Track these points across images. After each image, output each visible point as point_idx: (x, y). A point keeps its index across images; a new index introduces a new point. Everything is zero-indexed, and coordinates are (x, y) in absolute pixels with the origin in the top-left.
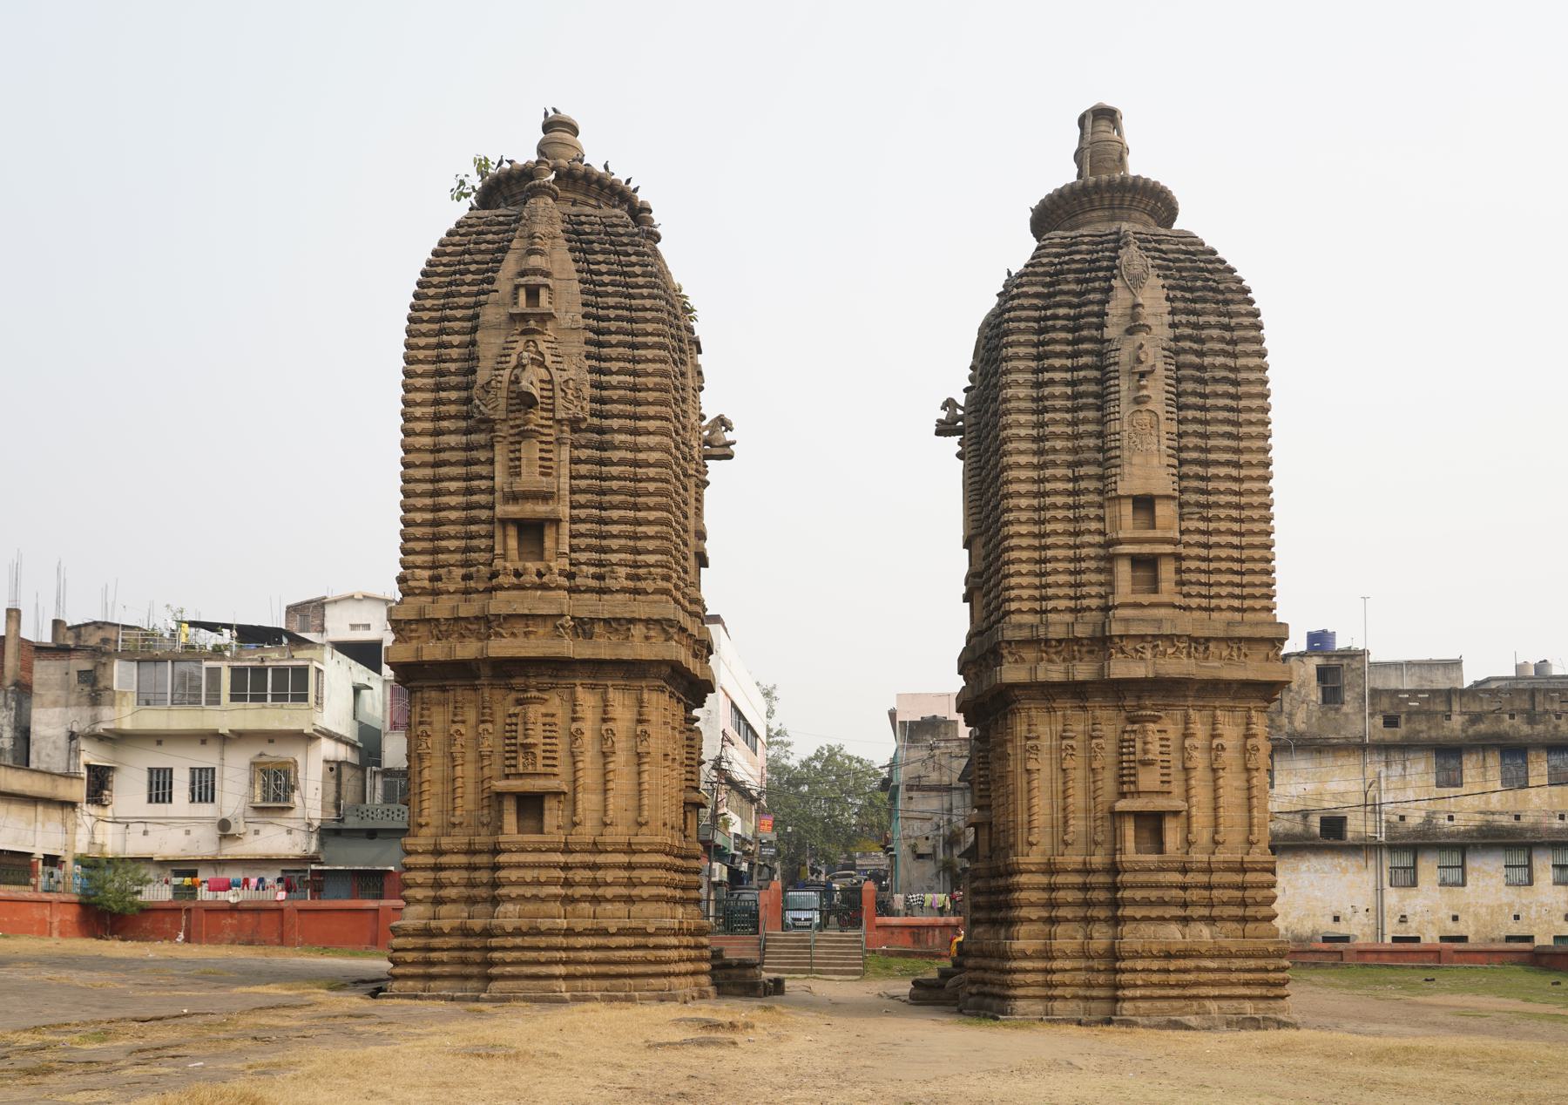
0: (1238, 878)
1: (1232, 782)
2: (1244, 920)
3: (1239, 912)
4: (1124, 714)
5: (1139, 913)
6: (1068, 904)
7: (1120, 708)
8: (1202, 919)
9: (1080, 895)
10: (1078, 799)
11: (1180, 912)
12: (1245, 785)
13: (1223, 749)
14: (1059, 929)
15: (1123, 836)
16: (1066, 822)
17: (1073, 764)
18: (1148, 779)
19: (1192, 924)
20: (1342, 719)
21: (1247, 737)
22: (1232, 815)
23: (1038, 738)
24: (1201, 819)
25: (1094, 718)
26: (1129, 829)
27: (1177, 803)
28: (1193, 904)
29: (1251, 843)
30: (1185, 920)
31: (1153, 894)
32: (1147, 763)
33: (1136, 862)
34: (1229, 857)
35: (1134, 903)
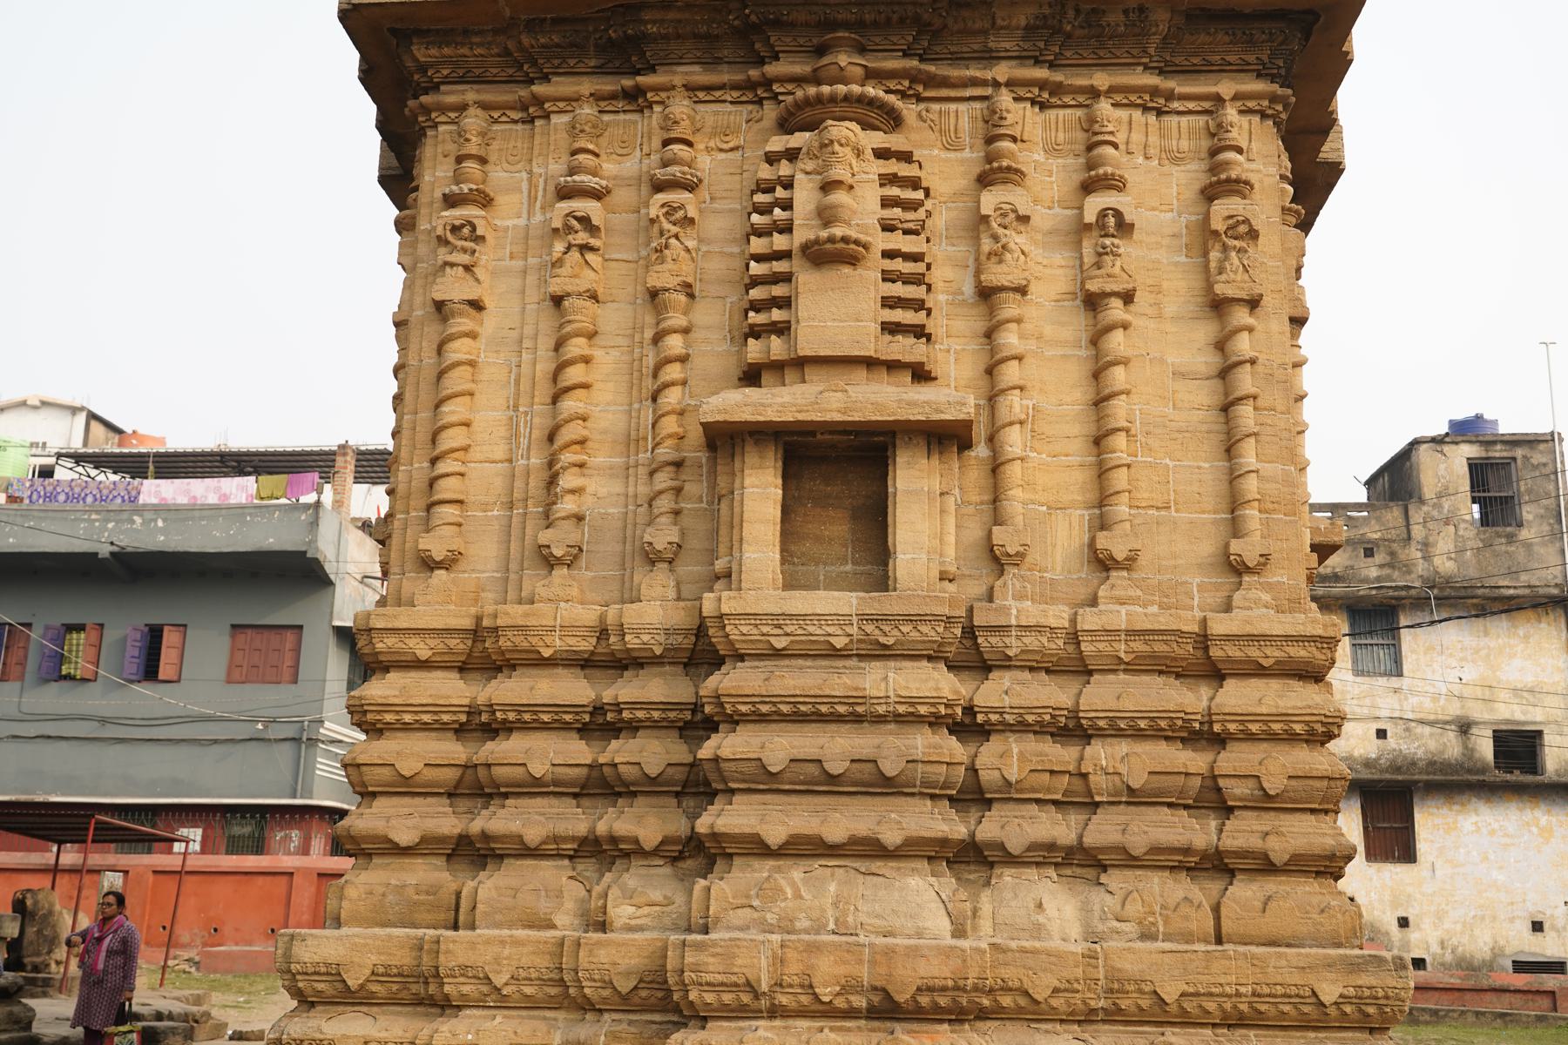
0: (1191, 699)
1: (1163, 349)
2: (1218, 865)
3: (1199, 832)
4: (770, 112)
5: (775, 820)
6: (533, 787)
7: (757, 91)
8: (1047, 856)
9: (578, 751)
10: (604, 403)
11: (949, 825)
13: (1125, 227)
14: (489, 886)
15: (736, 523)
16: (552, 481)
17: (587, 280)
18: (835, 312)
19: (1007, 877)
20: (1520, 554)
21: (1210, 194)
22: (1168, 469)
23: (485, 201)
25: (669, 122)
26: (761, 489)
27: (954, 396)
28: (1010, 794)
29: (1237, 569)
30: (972, 859)
31: (837, 747)
32: (830, 255)
33: (779, 620)
34: (1150, 616)
35: (764, 781)
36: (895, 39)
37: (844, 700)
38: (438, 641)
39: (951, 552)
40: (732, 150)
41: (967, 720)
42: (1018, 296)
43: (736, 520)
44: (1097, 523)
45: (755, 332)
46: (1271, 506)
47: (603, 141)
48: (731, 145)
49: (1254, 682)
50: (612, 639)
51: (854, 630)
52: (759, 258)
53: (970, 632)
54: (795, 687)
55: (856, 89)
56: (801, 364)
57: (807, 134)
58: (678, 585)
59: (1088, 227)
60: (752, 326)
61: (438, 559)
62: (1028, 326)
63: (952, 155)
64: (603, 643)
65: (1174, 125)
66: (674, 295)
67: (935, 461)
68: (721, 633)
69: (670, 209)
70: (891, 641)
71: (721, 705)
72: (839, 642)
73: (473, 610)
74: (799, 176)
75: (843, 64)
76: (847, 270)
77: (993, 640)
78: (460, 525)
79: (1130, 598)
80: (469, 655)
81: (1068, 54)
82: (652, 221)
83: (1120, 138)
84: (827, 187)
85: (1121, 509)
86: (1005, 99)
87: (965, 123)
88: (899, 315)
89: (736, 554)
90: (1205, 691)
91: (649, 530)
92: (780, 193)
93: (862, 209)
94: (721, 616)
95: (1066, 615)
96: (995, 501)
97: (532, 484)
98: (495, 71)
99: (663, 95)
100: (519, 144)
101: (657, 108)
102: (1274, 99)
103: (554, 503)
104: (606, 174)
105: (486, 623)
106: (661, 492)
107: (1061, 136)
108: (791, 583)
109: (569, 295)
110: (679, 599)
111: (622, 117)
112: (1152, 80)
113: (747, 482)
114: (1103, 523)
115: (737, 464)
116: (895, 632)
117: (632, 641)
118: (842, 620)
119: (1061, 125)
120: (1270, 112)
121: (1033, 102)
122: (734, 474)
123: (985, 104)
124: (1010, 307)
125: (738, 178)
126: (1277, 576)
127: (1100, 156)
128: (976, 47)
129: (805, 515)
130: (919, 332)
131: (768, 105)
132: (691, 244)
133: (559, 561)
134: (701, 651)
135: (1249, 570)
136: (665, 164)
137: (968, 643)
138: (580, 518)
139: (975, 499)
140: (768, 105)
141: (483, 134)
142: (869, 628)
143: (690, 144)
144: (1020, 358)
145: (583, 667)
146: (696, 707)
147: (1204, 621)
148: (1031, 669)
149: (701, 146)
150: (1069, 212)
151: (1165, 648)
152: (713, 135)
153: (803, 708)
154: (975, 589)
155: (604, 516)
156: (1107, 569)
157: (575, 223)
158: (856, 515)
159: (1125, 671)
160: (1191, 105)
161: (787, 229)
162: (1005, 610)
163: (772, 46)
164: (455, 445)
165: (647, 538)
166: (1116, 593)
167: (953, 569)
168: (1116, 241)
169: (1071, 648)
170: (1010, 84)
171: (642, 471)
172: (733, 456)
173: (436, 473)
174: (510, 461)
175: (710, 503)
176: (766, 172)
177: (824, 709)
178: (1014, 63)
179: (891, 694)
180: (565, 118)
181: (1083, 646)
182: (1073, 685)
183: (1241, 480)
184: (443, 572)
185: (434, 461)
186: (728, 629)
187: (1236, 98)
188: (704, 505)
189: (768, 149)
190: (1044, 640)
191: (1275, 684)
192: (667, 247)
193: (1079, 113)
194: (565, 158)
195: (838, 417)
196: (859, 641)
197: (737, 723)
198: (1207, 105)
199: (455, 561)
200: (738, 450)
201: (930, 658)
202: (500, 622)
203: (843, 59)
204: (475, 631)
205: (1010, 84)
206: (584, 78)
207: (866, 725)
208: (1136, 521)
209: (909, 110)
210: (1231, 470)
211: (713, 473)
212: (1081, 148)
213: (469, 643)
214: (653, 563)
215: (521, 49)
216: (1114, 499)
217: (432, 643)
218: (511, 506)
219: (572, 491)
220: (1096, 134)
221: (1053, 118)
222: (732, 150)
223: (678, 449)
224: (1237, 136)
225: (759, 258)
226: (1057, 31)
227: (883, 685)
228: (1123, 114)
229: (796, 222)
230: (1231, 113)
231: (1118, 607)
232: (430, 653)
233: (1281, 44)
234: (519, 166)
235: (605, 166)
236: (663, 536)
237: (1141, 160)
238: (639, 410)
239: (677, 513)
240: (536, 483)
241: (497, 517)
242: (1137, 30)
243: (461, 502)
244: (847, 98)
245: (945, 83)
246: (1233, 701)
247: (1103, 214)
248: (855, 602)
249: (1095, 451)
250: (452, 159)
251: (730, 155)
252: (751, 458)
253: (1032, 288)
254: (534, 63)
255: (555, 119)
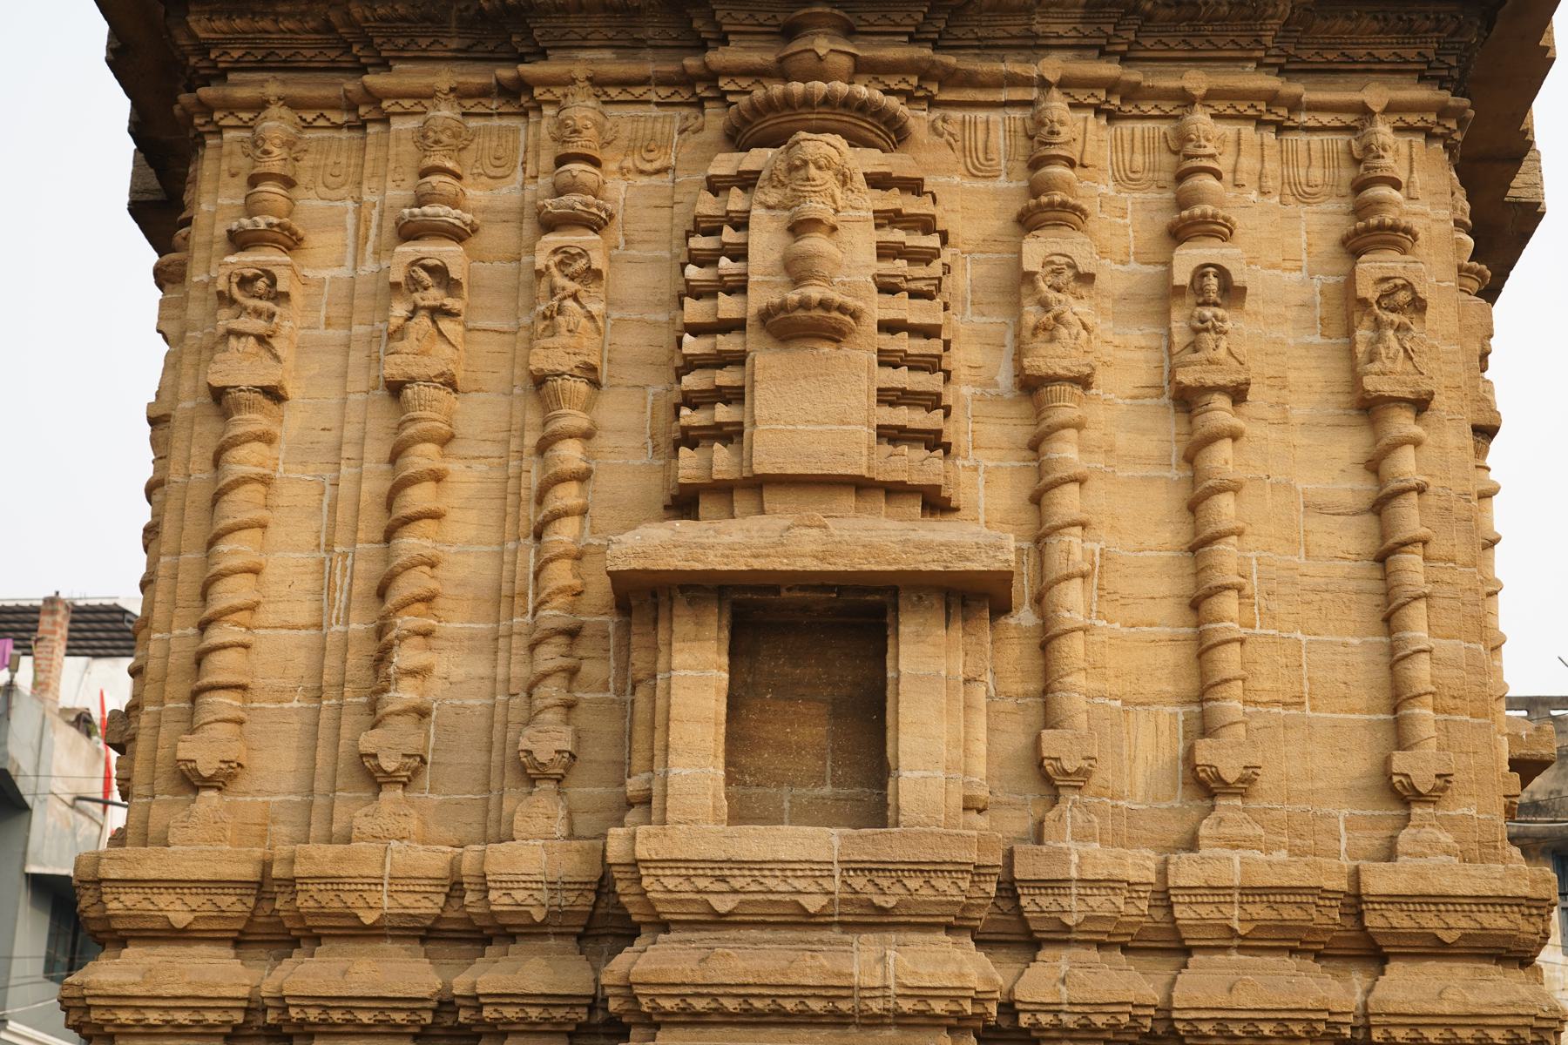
4: (715, 119)
7: (696, 88)
10: (463, 540)
12: (1352, 488)
13: (1232, 293)
15: (659, 723)
16: (382, 657)
17: (441, 358)
18: (810, 411)
21: (1355, 246)
23: (290, 241)
24: (1119, 646)
25: (567, 130)
27: (980, 536)
29: (1403, 796)
33: (722, 868)
34: (1276, 865)
36: (897, 18)
37: (819, 991)
38: (203, 899)
39: (980, 768)
40: (657, 172)
41: (1005, 1024)
42: (1078, 390)
43: (659, 718)
44: (1196, 725)
45: (690, 438)
46: (1451, 703)
47: (468, 157)
48: (657, 165)
49: (1431, 966)
50: (470, 897)
51: (835, 885)
52: (696, 330)
53: (1009, 888)
54: (746, 972)
55: (841, 87)
56: (758, 486)
57: (770, 152)
58: (570, 814)
59: (1179, 291)
60: (685, 430)
61: (206, 774)
62: (1092, 434)
63: (980, 184)
64: (455, 903)
65: (1302, 147)
66: (570, 383)
67: (957, 632)
68: (634, 889)
69: (566, 257)
70: (890, 902)
71: (634, 998)
72: (813, 904)
73: (258, 852)
74: (758, 213)
75: (822, 52)
76: (826, 349)
77: (1044, 902)
78: (241, 722)
79: (1246, 838)
80: (250, 921)
81: (1148, 43)
82: (539, 274)
83: (1224, 164)
84: (799, 228)
85: (1232, 705)
86: (1057, 105)
87: (999, 140)
88: (903, 416)
89: (659, 769)
90: (1358, 980)
91: (527, 731)
92: (729, 235)
93: (850, 261)
94: (635, 863)
95: (1152, 865)
96: (1046, 691)
97: (352, 660)
98: (309, 53)
99: (558, 92)
100: (343, 160)
101: (549, 111)
102: (1443, 112)
103: (385, 691)
104: (471, 204)
105: (277, 871)
106: (546, 675)
107: (1139, 159)
108: (739, 815)
109: (412, 380)
110: (571, 836)
111: (496, 122)
112: (1270, 82)
113: (677, 660)
114: (1205, 727)
115: (662, 635)
116: (898, 889)
117: (498, 900)
118: (818, 869)
119: (1138, 144)
120: (1439, 130)
121: (1098, 111)
122: (656, 649)
123: (1028, 112)
124: (1067, 405)
125: (667, 212)
126: (1462, 807)
127: (1196, 189)
128: (1015, 31)
129: (762, 711)
130: (933, 441)
131: (711, 109)
132: (596, 308)
133: (390, 779)
134: (604, 915)
135: (1420, 798)
136: (559, 192)
137: (1006, 905)
138: (422, 713)
139: (1016, 687)
140: (711, 109)
141: (289, 144)
142: (859, 882)
143: (596, 163)
144: (1080, 481)
145: (423, 940)
146: (595, 1002)
147: (1356, 875)
148: (1101, 945)
149: (613, 166)
150: (1150, 269)
151: (1300, 914)
152: (629, 150)
153: (758, 1004)
154: (1016, 823)
155: (459, 711)
156: (1211, 795)
157: (424, 275)
158: (838, 711)
159: (1240, 948)
160: (1326, 119)
161: (738, 287)
162: (1061, 856)
163: (718, 25)
164: (237, 601)
165: (525, 744)
166: (1226, 830)
167: (982, 793)
168: (1220, 312)
169: (1159, 914)
170: (1065, 84)
171: (519, 643)
172: (655, 621)
173: (206, 644)
174: (319, 626)
175: (620, 692)
176: (708, 205)
177: (789, 1005)
178: (1069, 54)
179: (891, 982)
180: (412, 123)
181: (1178, 911)
182: (1162, 969)
183: (1405, 664)
184: (213, 793)
185: (203, 626)
186: (645, 882)
187: (1390, 109)
188: (611, 695)
189: (711, 172)
190: (1120, 902)
191: (1462, 969)
192: (560, 311)
193: (1165, 127)
194: (411, 180)
195: (813, 565)
196: (844, 902)
197: (657, 1026)
198: (1348, 119)
199: (231, 777)
200: (663, 612)
201: (949, 929)
202: (298, 870)
203: (822, 45)
204: (260, 884)
205: (1065, 84)
206: (441, 66)
207: (852, 1030)
208: (1254, 724)
209: (918, 119)
210: (1392, 649)
211: (625, 647)
212: (1166, 177)
213: (251, 902)
214: (532, 781)
215: (350, 22)
216: (1221, 691)
217: (194, 902)
218: (319, 694)
219: (412, 673)
220: (1190, 157)
221: (1127, 133)
222: (657, 172)
223: (572, 610)
224: (1392, 164)
225: (696, 330)
226: (1135, 10)
227: (879, 969)
228: (1228, 129)
229: (752, 279)
230: (1383, 131)
231: (1228, 852)
232: (190, 917)
233: (1452, 35)
234: (343, 192)
235: (470, 192)
236: (549, 740)
237: (1254, 195)
238: (515, 552)
239: (570, 706)
240: (357, 662)
241: (297, 711)
242: (1247, 11)
243: (242, 688)
244: (828, 101)
245: (970, 80)
246: (1400, 995)
247: (1200, 272)
248: (836, 842)
249: (1191, 618)
250: (242, 180)
251: (655, 180)
252: (683, 624)
253: (1098, 379)
254: (368, 43)
255: (397, 124)
